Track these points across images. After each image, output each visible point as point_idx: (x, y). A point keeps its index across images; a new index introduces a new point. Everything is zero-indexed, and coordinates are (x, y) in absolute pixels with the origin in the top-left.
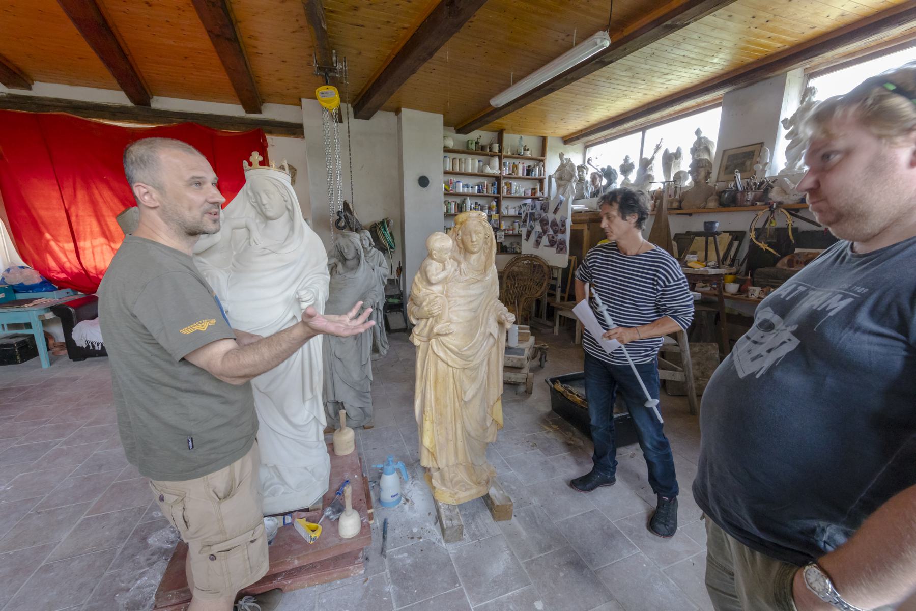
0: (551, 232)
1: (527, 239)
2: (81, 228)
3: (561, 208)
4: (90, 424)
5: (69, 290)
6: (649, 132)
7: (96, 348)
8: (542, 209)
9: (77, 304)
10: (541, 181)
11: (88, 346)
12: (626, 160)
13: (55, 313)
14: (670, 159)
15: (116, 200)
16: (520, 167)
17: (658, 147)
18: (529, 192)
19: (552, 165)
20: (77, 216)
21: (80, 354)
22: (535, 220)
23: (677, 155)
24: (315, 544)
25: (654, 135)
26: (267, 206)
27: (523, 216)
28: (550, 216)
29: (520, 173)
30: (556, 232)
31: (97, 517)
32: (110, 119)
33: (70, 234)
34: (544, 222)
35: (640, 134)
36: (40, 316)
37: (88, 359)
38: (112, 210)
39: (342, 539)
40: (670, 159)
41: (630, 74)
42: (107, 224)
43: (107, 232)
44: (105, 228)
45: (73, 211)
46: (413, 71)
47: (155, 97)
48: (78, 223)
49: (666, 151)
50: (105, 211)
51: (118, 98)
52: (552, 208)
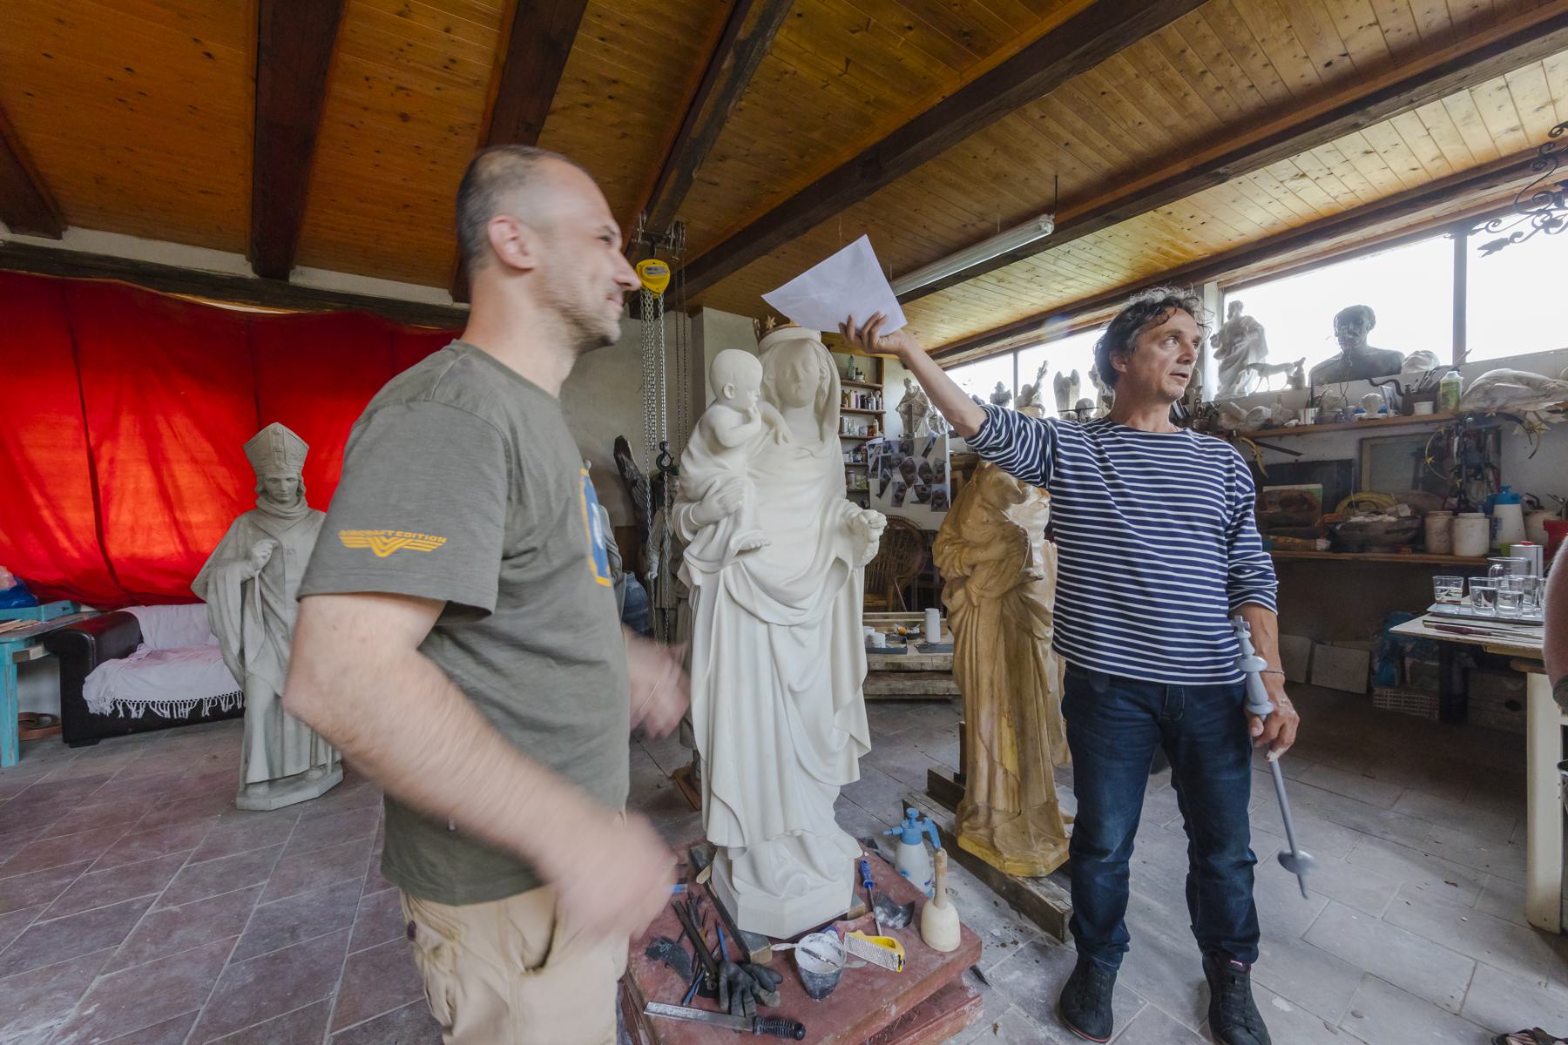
0: (920, 482)
1: (880, 496)
2: (117, 483)
3: (934, 448)
4: (199, 857)
5: (67, 603)
6: (1022, 354)
7: (134, 715)
8: (901, 450)
9: (95, 626)
10: (879, 416)
11: (116, 711)
12: (999, 386)
13: (47, 648)
14: (1064, 387)
15: (196, 433)
16: (853, 396)
17: (1042, 372)
18: (866, 431)
19: (893, 394)
20: (112, 461)
21: (80, 727)
22: (891, 467)
23: (1074, 379)
24: (907, 970)
25: (1030, 359)
26: (802, 384)
27: (871, 463)
28: (918, 460)
29: (853, 407)
30: (927, 482)
31: (364, 1028)
32: (208, 297)
33: (89, 495)
34: (907, 469)
35: (1011, 356)
36: (15, 655)
37: (104, 742)
38: (186, 449)
39: (942, 955)
40: (1064, 387)
41: (1029, 276)
42: (172, 476)
43: (171, 491)
44: (168, 481)
45: (106, 450)
46: (765, 252)
47: (298, 268)
48: (111, 474)
49: (1059, 374)
50: (172, 449)
51: (235, 265)
52: (919, 448)
